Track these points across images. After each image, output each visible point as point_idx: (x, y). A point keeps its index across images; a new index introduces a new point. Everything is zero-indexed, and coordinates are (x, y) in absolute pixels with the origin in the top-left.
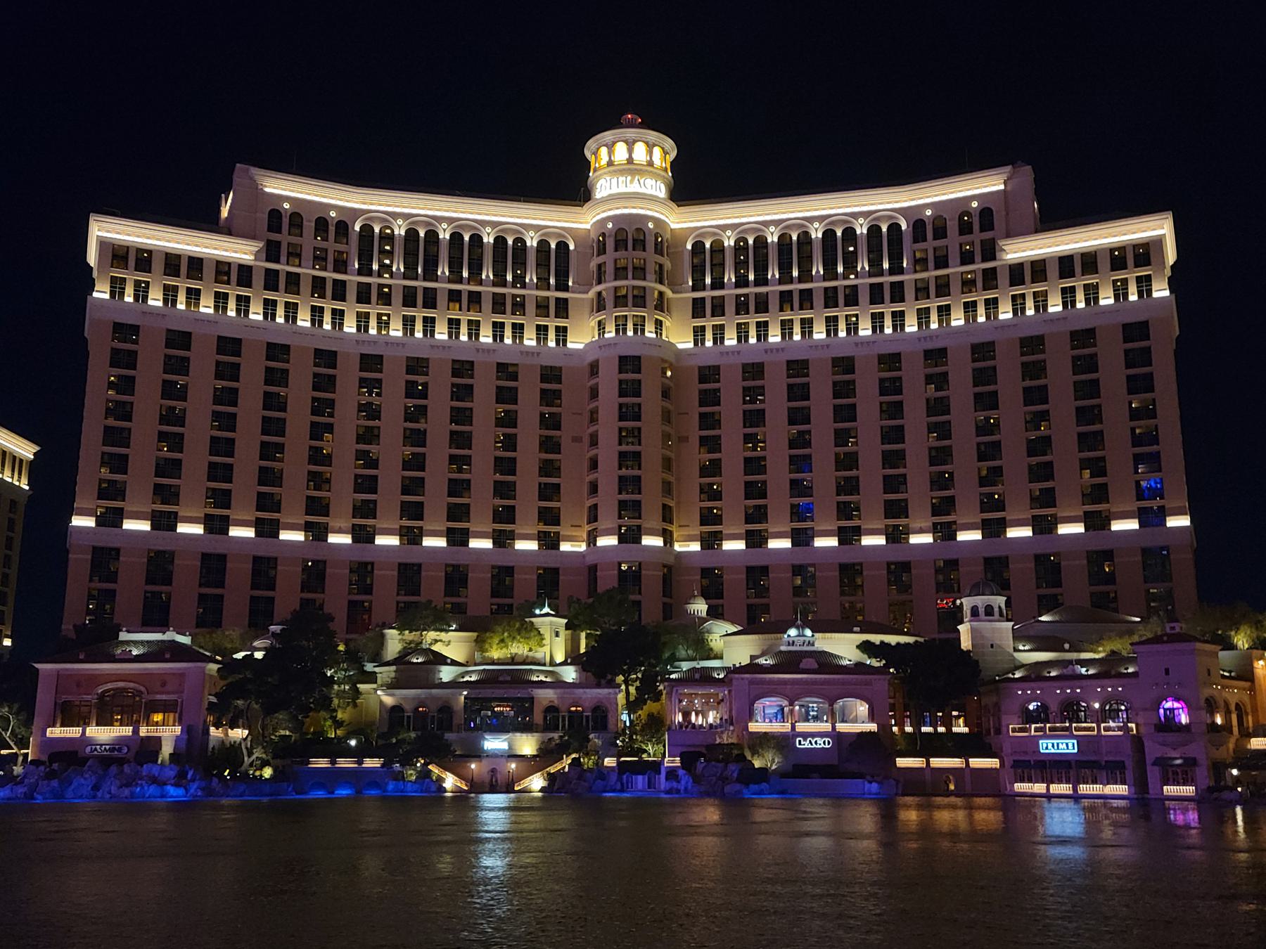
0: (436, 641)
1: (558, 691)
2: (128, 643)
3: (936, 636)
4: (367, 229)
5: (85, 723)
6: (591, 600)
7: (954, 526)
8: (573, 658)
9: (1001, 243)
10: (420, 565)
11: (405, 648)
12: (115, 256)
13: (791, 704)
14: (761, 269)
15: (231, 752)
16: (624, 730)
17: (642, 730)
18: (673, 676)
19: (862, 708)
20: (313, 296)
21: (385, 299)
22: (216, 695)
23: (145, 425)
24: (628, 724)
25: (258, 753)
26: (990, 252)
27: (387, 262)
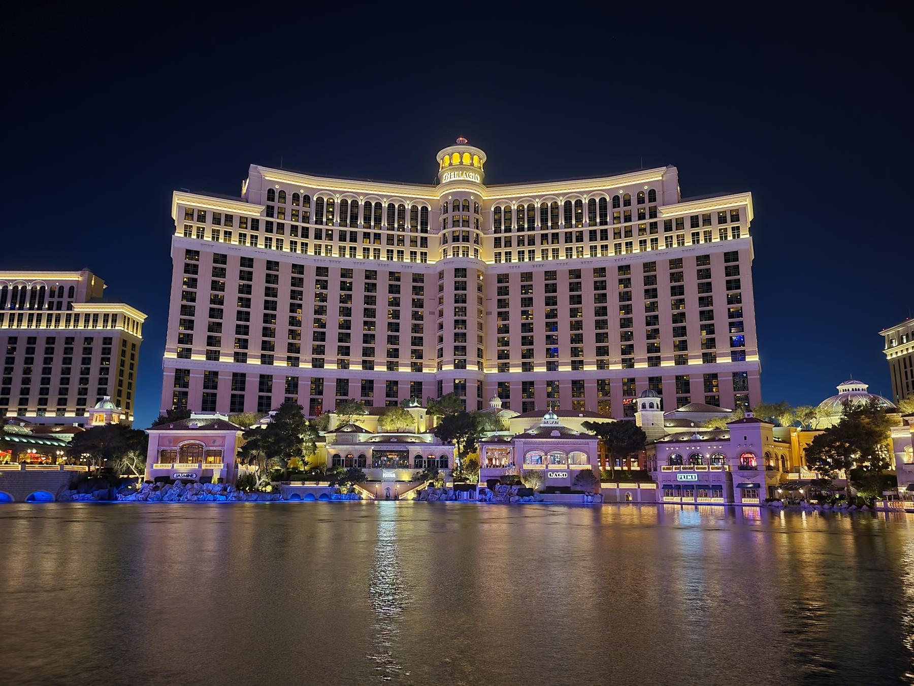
0: (357, 420)
1: (422, 447)
2: (195, 420)
3: (623, 419)
4: (320, 201)
5: (172, 460)
6: (439, 399)
7: (633, 361)
8: (431, 430)
9: (660, 208)
10: (348, 380)
11: (340, 424)
12: (187, 214)
13: (546, 454)
14: (531, 221)
15: (249, 480)
16: (457, 468)
17: (467, 468)
18: (483, 440)
19: (584, 457)
20: (291, 235)
21: (330, 237)
22: (242, 448)
23: (202, 305)
24: (459, 465)
25: (264, 478)
26: (653, 214)
27: (331, 217)
